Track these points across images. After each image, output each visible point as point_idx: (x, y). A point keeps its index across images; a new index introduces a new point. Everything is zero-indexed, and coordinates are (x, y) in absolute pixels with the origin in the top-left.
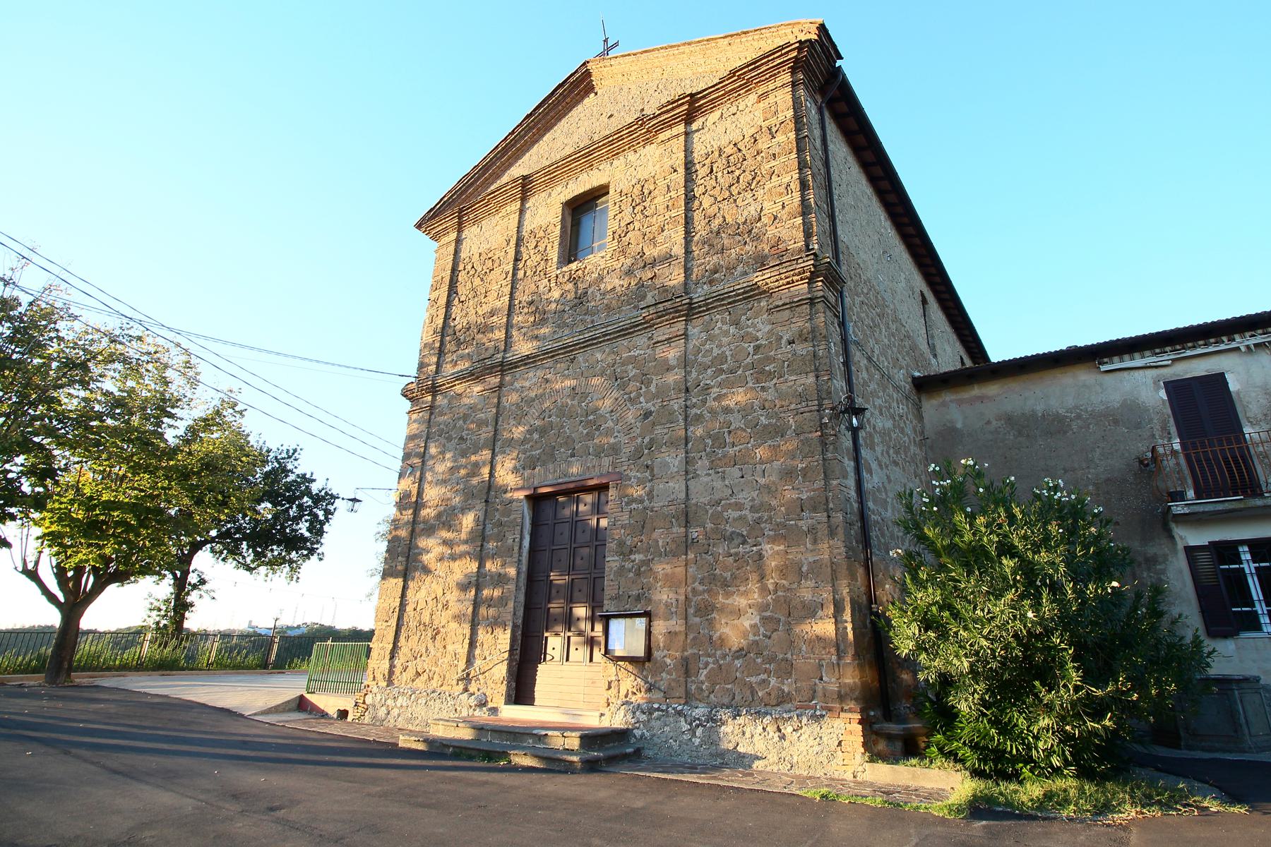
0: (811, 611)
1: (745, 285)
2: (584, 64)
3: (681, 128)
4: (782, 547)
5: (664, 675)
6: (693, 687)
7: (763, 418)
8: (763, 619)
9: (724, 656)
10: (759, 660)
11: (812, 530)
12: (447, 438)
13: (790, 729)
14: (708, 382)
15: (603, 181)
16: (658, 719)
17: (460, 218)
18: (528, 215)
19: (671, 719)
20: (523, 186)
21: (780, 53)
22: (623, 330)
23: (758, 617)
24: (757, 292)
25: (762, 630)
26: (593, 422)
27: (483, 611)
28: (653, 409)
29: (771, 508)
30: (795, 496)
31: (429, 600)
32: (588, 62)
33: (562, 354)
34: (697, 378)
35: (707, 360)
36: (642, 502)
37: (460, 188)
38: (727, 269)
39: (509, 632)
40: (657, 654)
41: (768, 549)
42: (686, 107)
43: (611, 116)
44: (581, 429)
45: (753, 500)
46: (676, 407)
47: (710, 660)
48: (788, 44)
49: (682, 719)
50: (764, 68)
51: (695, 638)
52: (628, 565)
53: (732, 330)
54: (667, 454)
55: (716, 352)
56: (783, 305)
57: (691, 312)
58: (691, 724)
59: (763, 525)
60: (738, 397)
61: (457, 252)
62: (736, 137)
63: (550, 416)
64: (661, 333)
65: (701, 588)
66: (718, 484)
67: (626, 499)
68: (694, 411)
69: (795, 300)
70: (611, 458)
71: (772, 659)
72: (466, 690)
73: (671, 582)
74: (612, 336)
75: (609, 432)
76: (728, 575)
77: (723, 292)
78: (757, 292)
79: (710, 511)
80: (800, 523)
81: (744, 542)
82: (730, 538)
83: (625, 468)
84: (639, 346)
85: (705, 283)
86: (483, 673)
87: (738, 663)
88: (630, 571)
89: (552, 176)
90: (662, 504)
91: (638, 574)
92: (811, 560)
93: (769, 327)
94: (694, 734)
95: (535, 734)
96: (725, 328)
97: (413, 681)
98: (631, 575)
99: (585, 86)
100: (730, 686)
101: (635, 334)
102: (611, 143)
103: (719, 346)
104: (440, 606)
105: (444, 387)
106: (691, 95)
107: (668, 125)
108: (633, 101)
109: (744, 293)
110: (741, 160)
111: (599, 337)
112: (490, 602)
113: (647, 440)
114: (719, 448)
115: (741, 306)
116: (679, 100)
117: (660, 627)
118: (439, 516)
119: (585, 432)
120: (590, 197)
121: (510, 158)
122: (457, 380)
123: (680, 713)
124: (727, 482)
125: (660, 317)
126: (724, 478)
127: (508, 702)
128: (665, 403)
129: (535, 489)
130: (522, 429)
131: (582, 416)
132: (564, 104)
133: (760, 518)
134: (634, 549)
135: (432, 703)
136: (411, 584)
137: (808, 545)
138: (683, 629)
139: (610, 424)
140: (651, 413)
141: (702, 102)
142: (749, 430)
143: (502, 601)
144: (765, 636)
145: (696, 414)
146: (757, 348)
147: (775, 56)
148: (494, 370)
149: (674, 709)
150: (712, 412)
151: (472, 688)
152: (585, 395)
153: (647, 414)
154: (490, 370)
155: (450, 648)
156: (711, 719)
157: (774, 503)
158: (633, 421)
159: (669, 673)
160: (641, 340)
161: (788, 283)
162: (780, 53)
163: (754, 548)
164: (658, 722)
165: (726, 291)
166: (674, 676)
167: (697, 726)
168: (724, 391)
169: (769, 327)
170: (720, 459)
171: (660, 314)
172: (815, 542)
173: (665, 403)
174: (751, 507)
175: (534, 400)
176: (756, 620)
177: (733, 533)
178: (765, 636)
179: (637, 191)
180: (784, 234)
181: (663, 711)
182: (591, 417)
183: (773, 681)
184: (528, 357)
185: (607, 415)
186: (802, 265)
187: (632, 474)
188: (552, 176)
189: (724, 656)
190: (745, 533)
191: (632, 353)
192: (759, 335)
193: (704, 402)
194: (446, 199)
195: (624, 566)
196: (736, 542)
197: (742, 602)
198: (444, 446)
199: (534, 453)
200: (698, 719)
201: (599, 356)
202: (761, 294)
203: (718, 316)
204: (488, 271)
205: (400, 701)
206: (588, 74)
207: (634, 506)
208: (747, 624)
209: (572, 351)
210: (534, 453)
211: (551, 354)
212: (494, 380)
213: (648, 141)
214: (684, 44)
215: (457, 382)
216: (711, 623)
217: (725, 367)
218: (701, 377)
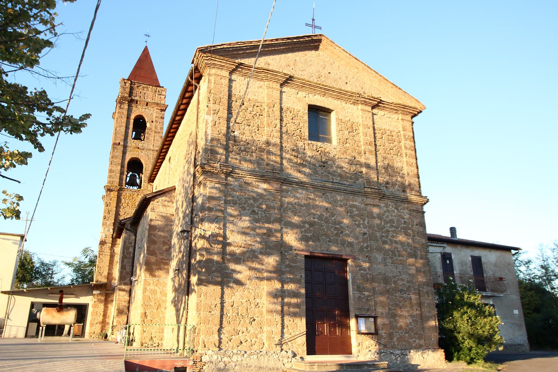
0: (428, 319)
1: (404, 197)
2: (321, 35)
3: (369, 109)
4: (417, 297)
5: (383, 339)
6: (392, 344)
7: (409, 249)
8: (413, 320)
9: (402, 333)
10: (412, 334)
11: (427, 292)
12: (241, 208)
13: (426, 356)
14: (389, 229)
15: (331, 107)
16: (384, 356)
17: (237, 67)
18: (284, 95)
19: (389, 355)
20: (287, 79)
21: (413, 109)
22: (354, 192)
23: (411, 320)
24: (406, 201)
25: (413, 324)
26: (340, 230)
27: (286, 308)
28: (367, 232)
29: (413, 283)
30: (422, 280)
31: (244, 301)
32: (323, 36)
33: (320, 189)
34: (384, 225)
35: (388, 220)
36: (366, 270)
37: (236, 47)
38: (392, 185)
39: (304, 320)
40: (380, 332)
41: (413, 297)
42: (376, 103)
43: (329, 73)
44: (332, 230)
45: (407, 278)
46: (378, 235)
47: (398, 334)
48: (417, 109)
49: (393, 355)
50: (406, 110)
51: (391, 327)
52: (362, 296)
53: (396, 211)
54: (376, 253)
55: (390, 217)
56: (416, 210)
57: (383, 197)
58: (396, 356)
59: (411, 288)
60: (401, 238)
61: (230, 87)
62: (391, 129)
63: (314, 218)
64: (369, 201)
65: (393, 308)
66: (394, 270)
67: (359, 268)
68: (384, 239)
69: (420, 210)
70: (350, 248)
71: (416, 334)
72: (282, 350)
73: (383, 305)
74: (347, 192)
75: (347, 235)
76: (401, 304)
77: (396, 195)
78: (406, 201)
79: (393, 280)
80: (424, 289)
81: (405, 293)
82: (401, 291)
83: (357, 254)
84: (357, 202)
85: (384, 186)
86: (290, 341)
87: (407, 335)
88: (364, 298)
89: (304, 85)
90: (376, 273)
91: (367, 300)
92: (428, 302)
93: (408, 216)
94: (397, 360)
95: (368, 365)
96: (393, 209)
97: (238, 346)
98: (364, 300)
99: (316, 45)
100: (404, 343)
101: (357, 195)
102: (340, 93)
103: (392, 216)
104: (253, 305)
105: (238, 175)
106: (381, 100)
107: (365, 103)
108: (341, 74)
109: (402, 199)
110: (393, 141)
111: (342, 190)
112: (289, 305)
113: (365, 245)
114: (394, 256)
115: (399, 203)
116: (377, 99)
117: (379, 321)
118: (243, 253)
119: (335, 232)
120: (323, 110)
121: (268, 51)
122: (249, 175)
123: (392, 353)
124: (398, 270)
125: (371, 194)
126: (397, 268)
127: (308, 354)
128: (374, 232)
129: (311, 253)
130: (297, 219)
131: (333, 224)
132: (304, 45)
133: (410, 285)
134: (364, 290)
135: (262, 357)
136: (227, 291)
137: (426, 297)
138: (389, 323)
139: (347, 232)
140: (366, 234)
141: (381, 105)
142: (404, 253)
143: (297, 305)
144: (414, 326)
145: (384, 240)
146: (405, 222)
147: (412, 109)
148: (278, 181)
149: (389, 352)
150: (391, 240)
151: (284, 347)
152: (333, 215)
153: (365, 234)
154: (278, 180)
155: (265, 329)
156: (402, 354)
157: (414, 281)
158: (359, 234)
159: (384, 339)
160: (360, 199)
161: (417, 203)
162: (413, 109)
163: (409, 296)
164: (384, 357)
165: (398, 195)
166: (386, 340)
167: (398, 357)
168: (395, 235)
169: (408, 216)
170: (395, 261)
171: (372, 193)
172: (428, 296)
173: (374, 232)
174: (407, 281)
175: (303, 207)
176: (411, 321)
177: (401, 289)
178: (414, 326)
179: (349, 124)
180: (412, 182)
181: (385, 353)
182: (337, 226)
183: (417, 341)
184: (302, 182)
185: (346, 228)
186: (424, 199)
187: (360, 258)
188: (304, 85)
189: (402, 333)
190: (405, 290)
191: (354, 203)
192: (405, 217)
193: (387, 236)
194: (225, 46)
195: (360, 296)
196: (403, 292)
197: (405, 313)
198: (240, 211)
199: (307, 234)
200: (398, 355)
201: (339, 198)
202: (406, 202)
203: (390, 203)
204: (258, 114)
205: (235, 358)
206: (320, 41)
207: (362, 271)
208: (408, 322)
209: (325, 190)
210: (307, 234)
211: (314, 187)
212: (276, 186)
213: (354, 103)
214: (374, 71)
215: (248, 176)
216: (397, 321)
217: (394, 225)
218: (385, 226)
